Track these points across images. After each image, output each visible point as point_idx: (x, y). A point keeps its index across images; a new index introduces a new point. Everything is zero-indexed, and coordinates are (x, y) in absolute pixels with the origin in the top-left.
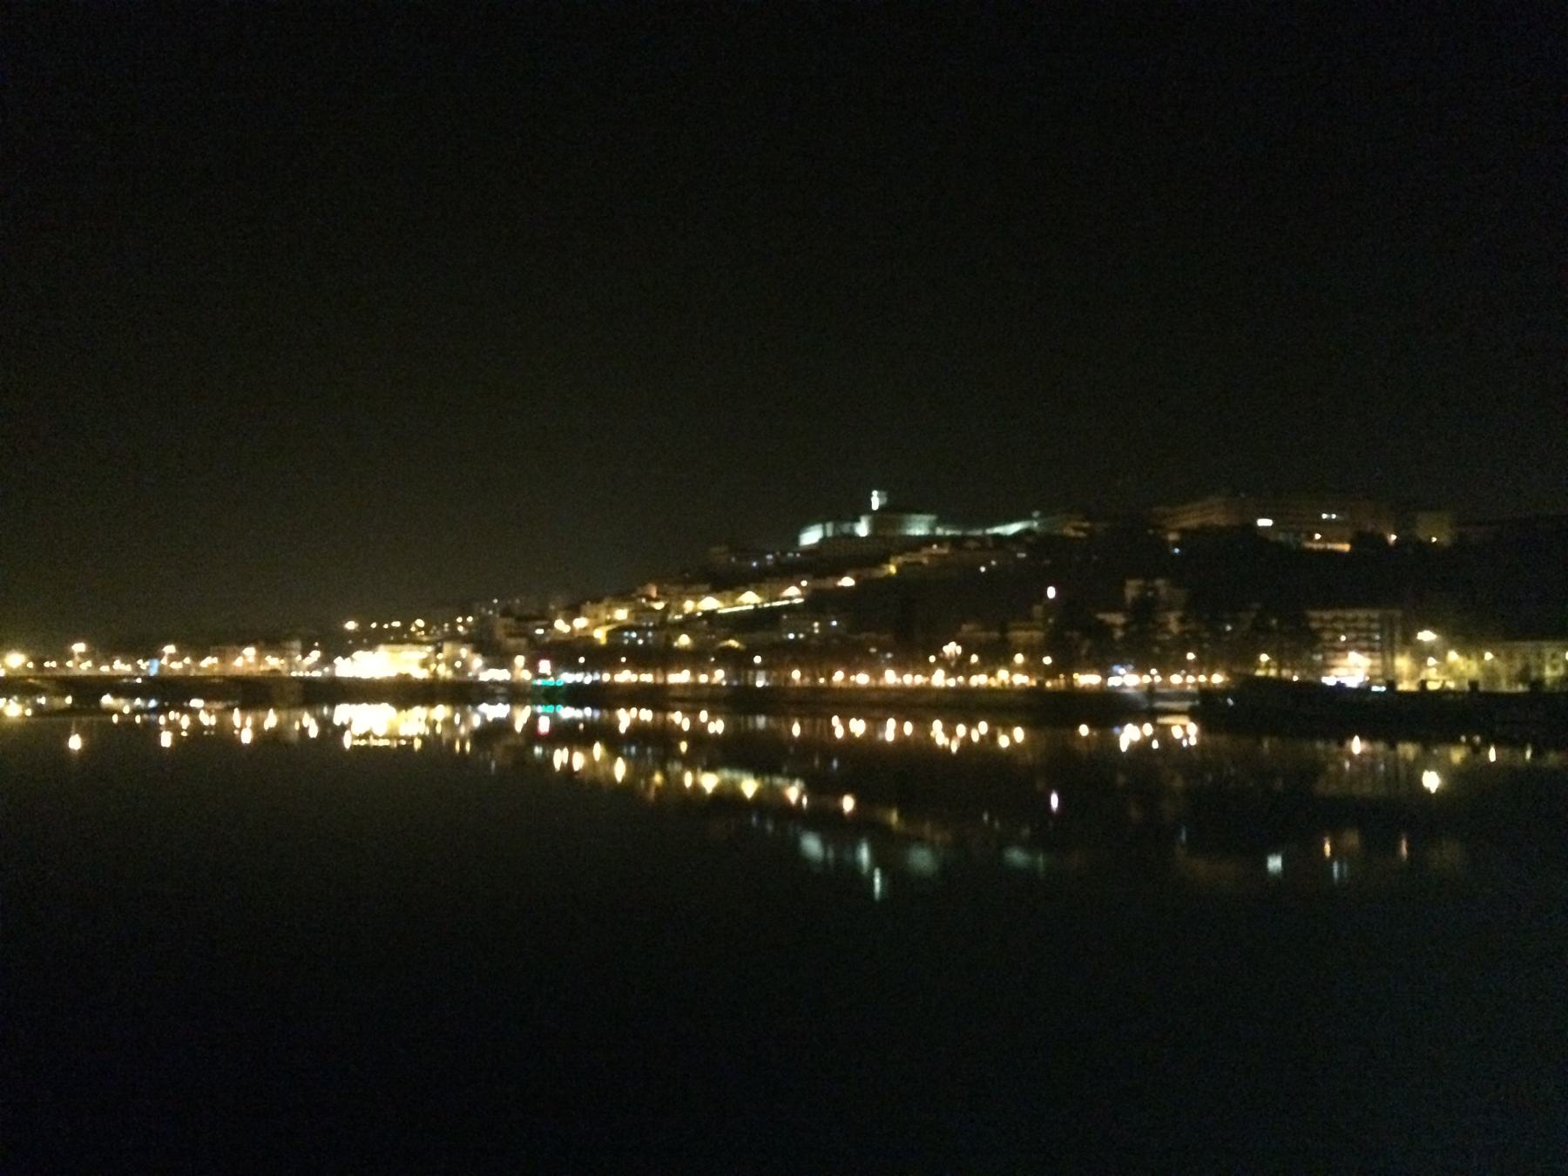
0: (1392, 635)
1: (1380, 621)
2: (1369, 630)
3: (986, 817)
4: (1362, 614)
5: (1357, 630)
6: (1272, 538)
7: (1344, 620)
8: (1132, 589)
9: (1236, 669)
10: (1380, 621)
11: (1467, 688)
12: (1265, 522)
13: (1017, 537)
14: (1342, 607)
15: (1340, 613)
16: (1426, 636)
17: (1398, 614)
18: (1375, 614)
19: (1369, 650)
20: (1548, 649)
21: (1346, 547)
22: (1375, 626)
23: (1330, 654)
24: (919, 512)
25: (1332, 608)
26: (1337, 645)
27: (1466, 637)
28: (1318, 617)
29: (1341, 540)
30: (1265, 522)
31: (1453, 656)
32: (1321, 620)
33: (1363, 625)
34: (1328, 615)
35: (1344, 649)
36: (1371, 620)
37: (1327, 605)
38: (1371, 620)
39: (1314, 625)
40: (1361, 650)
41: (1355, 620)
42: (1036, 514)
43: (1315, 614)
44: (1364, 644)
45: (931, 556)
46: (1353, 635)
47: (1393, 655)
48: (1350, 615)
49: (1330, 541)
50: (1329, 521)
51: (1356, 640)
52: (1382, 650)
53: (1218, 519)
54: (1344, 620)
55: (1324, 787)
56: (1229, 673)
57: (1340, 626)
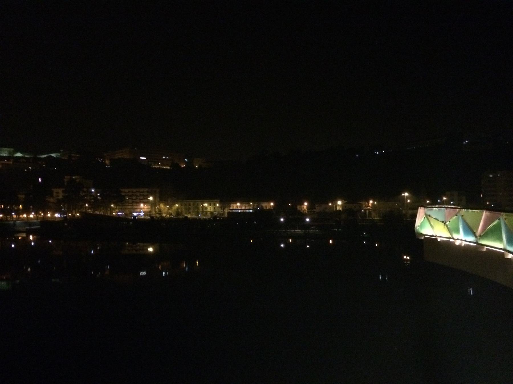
3: (25, 268)
4: (146, 190)
5: (144, 195)
7: (139, 192)
8: (67, 178)
13: (45, 157)
15: (137, 190)
16: (151, 198)
24: (6, 147)
29: (167, 165)
34: (134, 190)
41: (143, 192)
42: (62, 151)
43: (121, 190)
45: (3, 164)
48: (142, 190)
49: (165, 166)
53: (126, 156)
54: (139, 192)
57: (138, 194)
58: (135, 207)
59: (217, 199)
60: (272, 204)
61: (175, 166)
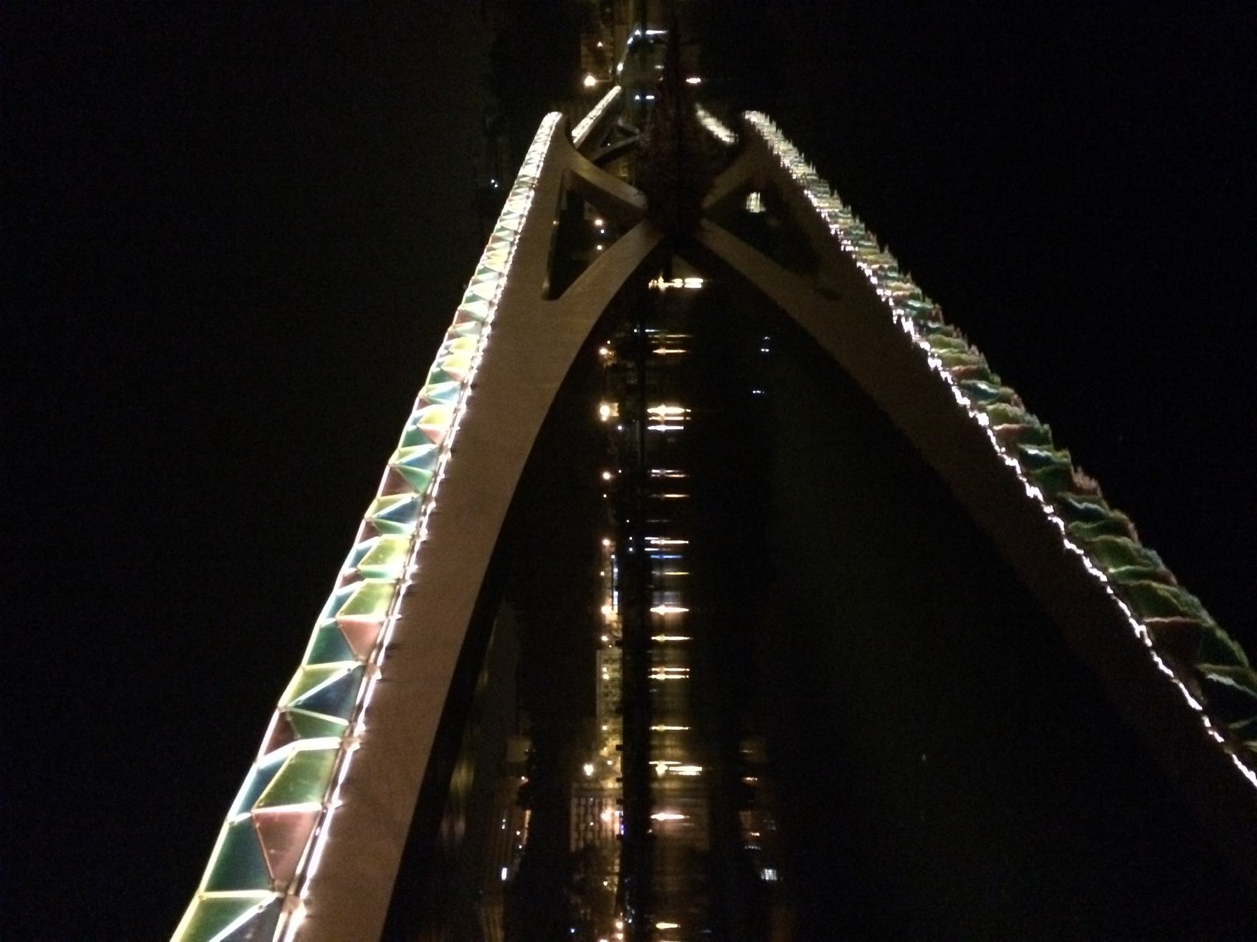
0: (590, 790)
1: (579, 797)
2: (586, 807)
4: (574, 811)
5: (586, 814)
6: (517, 869)
7: (578, 825)
9: (612, 912)
10: (579, 797)
11: (620, 753)
12: (504, 874)
14: (568, 824)
15: (573, 827)
16: (589, 769)
17: (575, 785)
18: (575, 801)
19: (601, 807)
20: (600, 690)
21: (528, 813)
22: (583, 801)
23: (603, 834)
25: (568, 831)
26: (597, 827)
27: (590, 746)
28: (575, 845)
29: (523, 818)
30: (504, 874)
31: (605, 752)
32: (578, 840)
33: (582, 811)
34: (574, 835)
35: (599, 822)
36: (579, 804)
37: (568, 837)
38: (579, 804)
39: (582, 844)
40: (601, 810)
41: (578, 815)
43: (573, 847)
44: (597, 809)
46: (590, 817)
47: (602, 789)
48: (574, 819)
50: (508, 824)
51: (594, 816)
52: (601, 797)
54: (578, 825)
55: (703, 845)
56: (616, 916)
57: (582, 826)
58: (610, 834)
59: (595, 657)
60: (606, 542)
61: (525, 798)
